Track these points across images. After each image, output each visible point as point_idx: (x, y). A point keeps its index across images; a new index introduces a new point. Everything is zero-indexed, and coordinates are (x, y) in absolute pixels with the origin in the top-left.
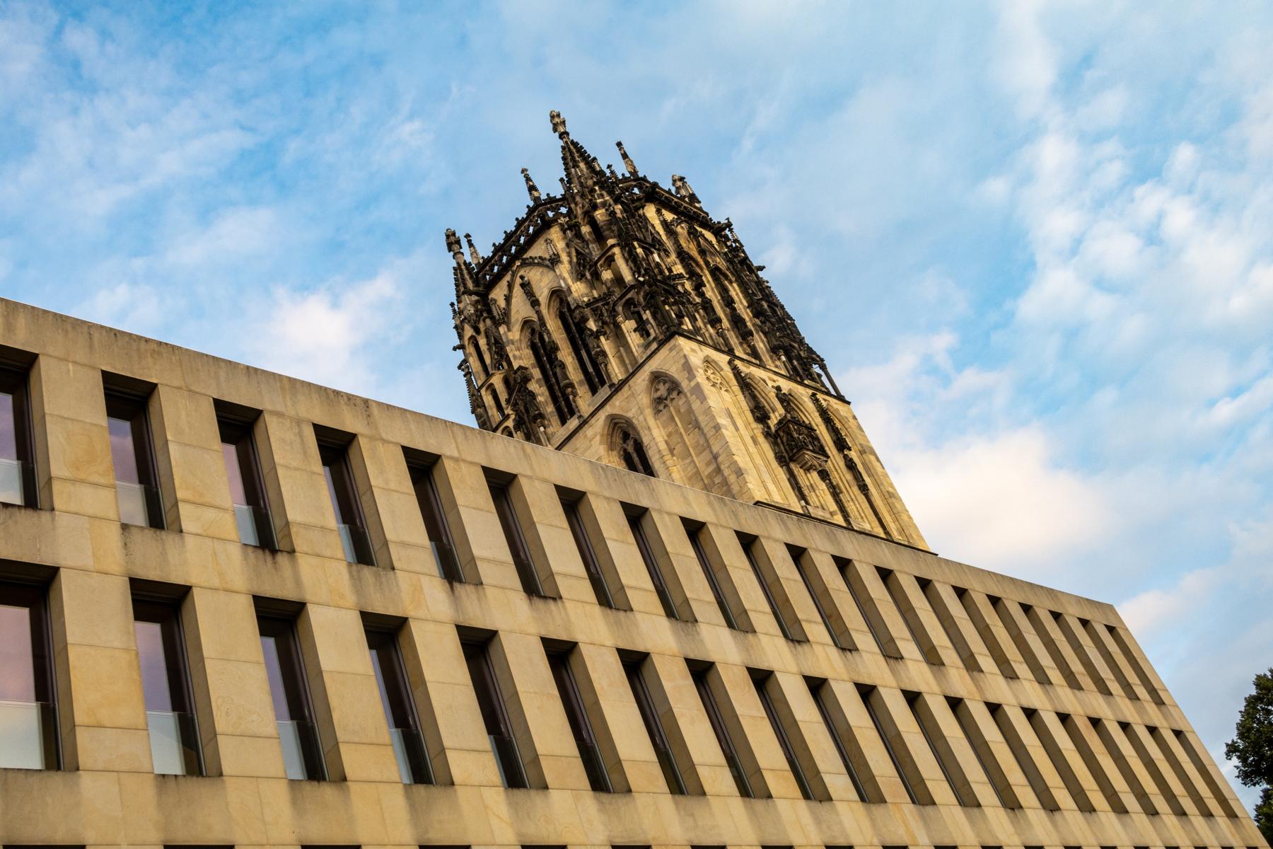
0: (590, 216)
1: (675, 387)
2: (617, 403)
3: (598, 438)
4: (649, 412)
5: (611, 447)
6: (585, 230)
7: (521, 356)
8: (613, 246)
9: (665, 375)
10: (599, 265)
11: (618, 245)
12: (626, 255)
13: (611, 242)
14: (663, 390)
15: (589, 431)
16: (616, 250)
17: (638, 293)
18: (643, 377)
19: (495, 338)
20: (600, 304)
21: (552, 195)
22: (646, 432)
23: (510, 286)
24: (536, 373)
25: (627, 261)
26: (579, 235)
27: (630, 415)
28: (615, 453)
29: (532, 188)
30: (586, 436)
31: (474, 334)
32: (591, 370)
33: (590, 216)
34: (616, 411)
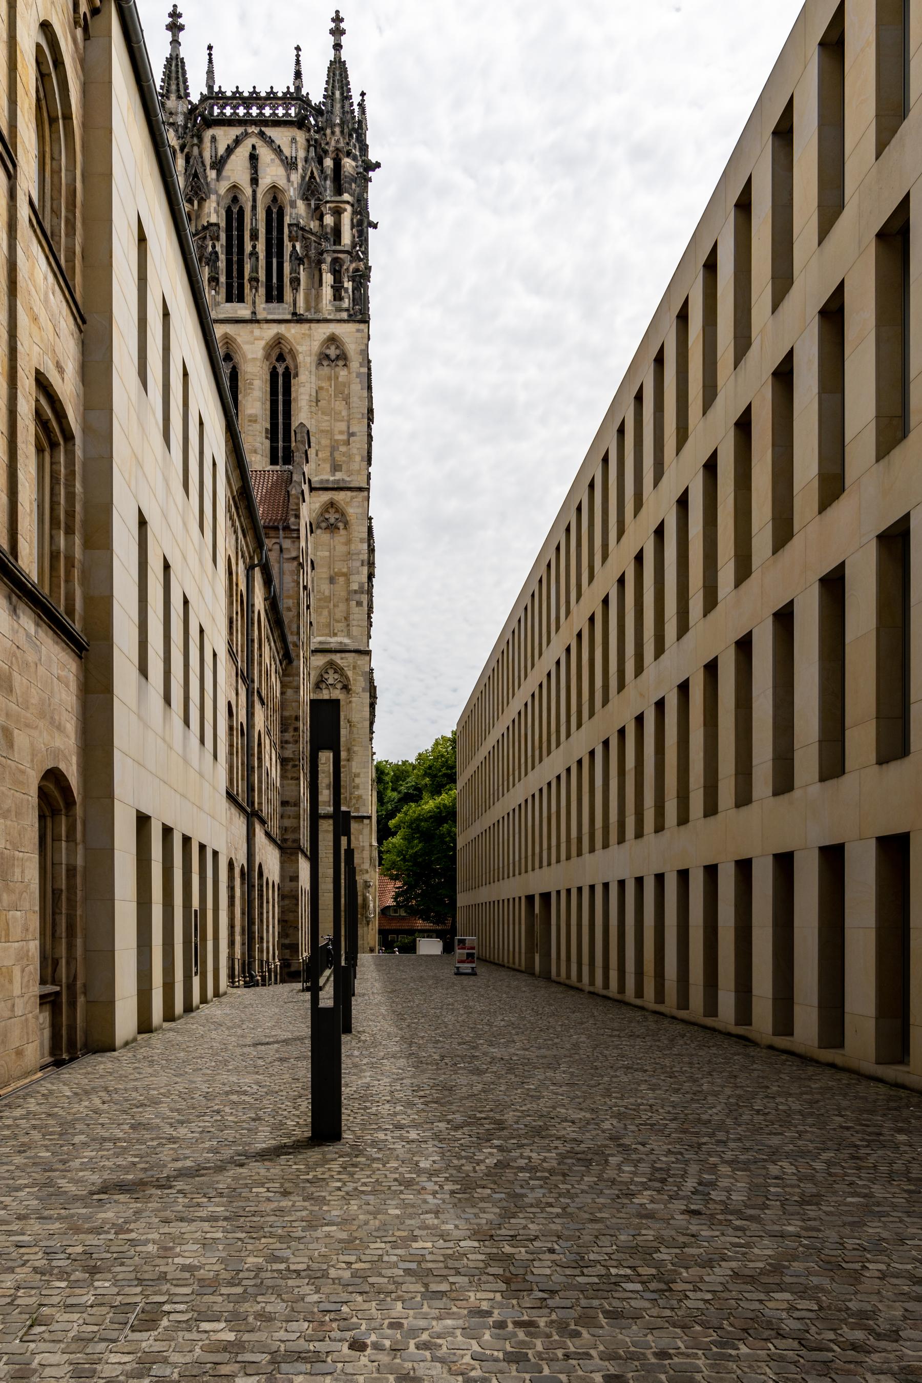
0: (337, 155)
1: (343, 357)
2: (293, 331)
3: (262, 343)
4: (314, 358)
5: (267, 357)
6: (328, 162)
7: (213, 212)
8: (348, 202)
9: (343, 344)
10: (328, 205)
11: (352, 206)
12: (355, 221)
13: (346, 197)
15: (256, 330)
16: (349, 208)
17: (351, 262)
18: (325, 331)
19: (196, 171)
20: (313, 238)
21: (310, 97)
22: (307, 373)
23: (237, 141)
24: (223, 236)
25: (352, 227)
26: (320, 162)
27: (300, 349)
28: (268, 363)
29: (298, 75)
30: (252, 332)
31: (177, 148)
32: (275, 280)
33: (337, 155)
34: (288, 335)
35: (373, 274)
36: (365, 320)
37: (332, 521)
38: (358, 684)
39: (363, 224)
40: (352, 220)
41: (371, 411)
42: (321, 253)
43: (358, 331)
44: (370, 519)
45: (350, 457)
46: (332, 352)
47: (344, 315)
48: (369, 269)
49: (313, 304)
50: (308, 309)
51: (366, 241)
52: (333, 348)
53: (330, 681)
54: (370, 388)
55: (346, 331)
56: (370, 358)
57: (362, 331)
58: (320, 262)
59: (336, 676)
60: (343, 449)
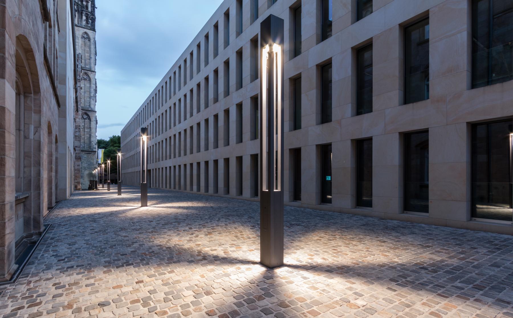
11: (91, 2)
14: (85, 36)
25: (91, 7)
35: (96, 19)
36: (94, 30)
37: (85, 78)
38: (93, 119)
39: (94, 7)
40: (91, 5)
41: (96, 53)
42: (82, 11)
43: (93, 33)
44: (96, 79)
45: (90, 63)
46: (85, 36)
47: (89, 28)
48: (95, 18)
49: (80, 23)
50: (78, 23)
51: (94, 12)
52: (86, 35)
53: (85, 117)
54: (96, 48)
55: (90, 32)
56: (96, 40)
57: (94, 33)
58: (82, 13)
59: (87, 116)
60: (88, 61)
